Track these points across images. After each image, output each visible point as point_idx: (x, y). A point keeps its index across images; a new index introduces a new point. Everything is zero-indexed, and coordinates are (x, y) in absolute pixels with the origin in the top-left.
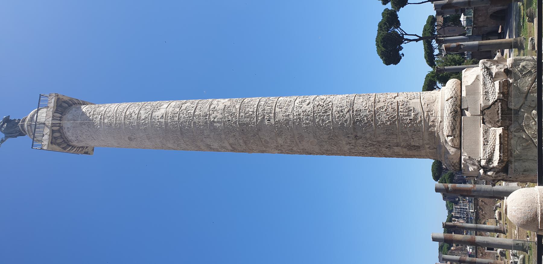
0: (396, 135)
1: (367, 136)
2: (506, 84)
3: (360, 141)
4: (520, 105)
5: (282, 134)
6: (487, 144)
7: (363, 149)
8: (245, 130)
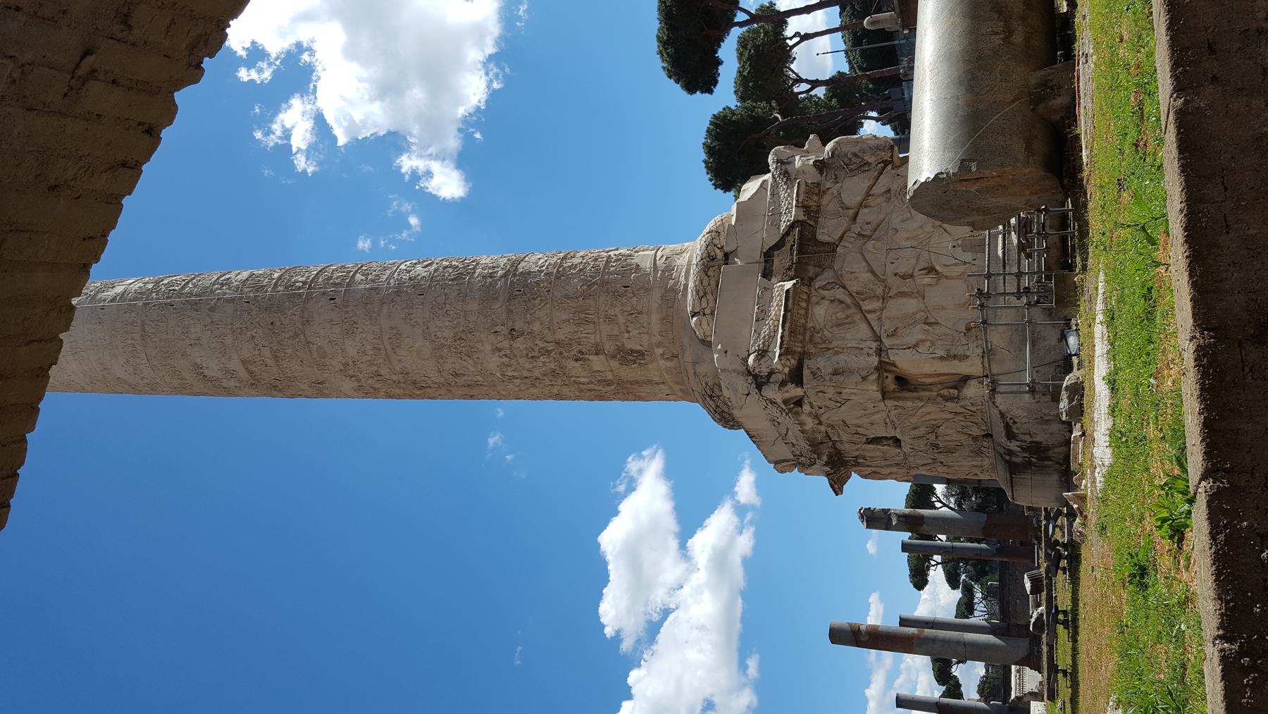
0: (594, 323)
1: (535, 329)
2: (817, 192)
3: (520, 344)
4: (841, 232)
5: (355, 330)
6: (763, 319)
7: (527, 366)
8: (278, 324)
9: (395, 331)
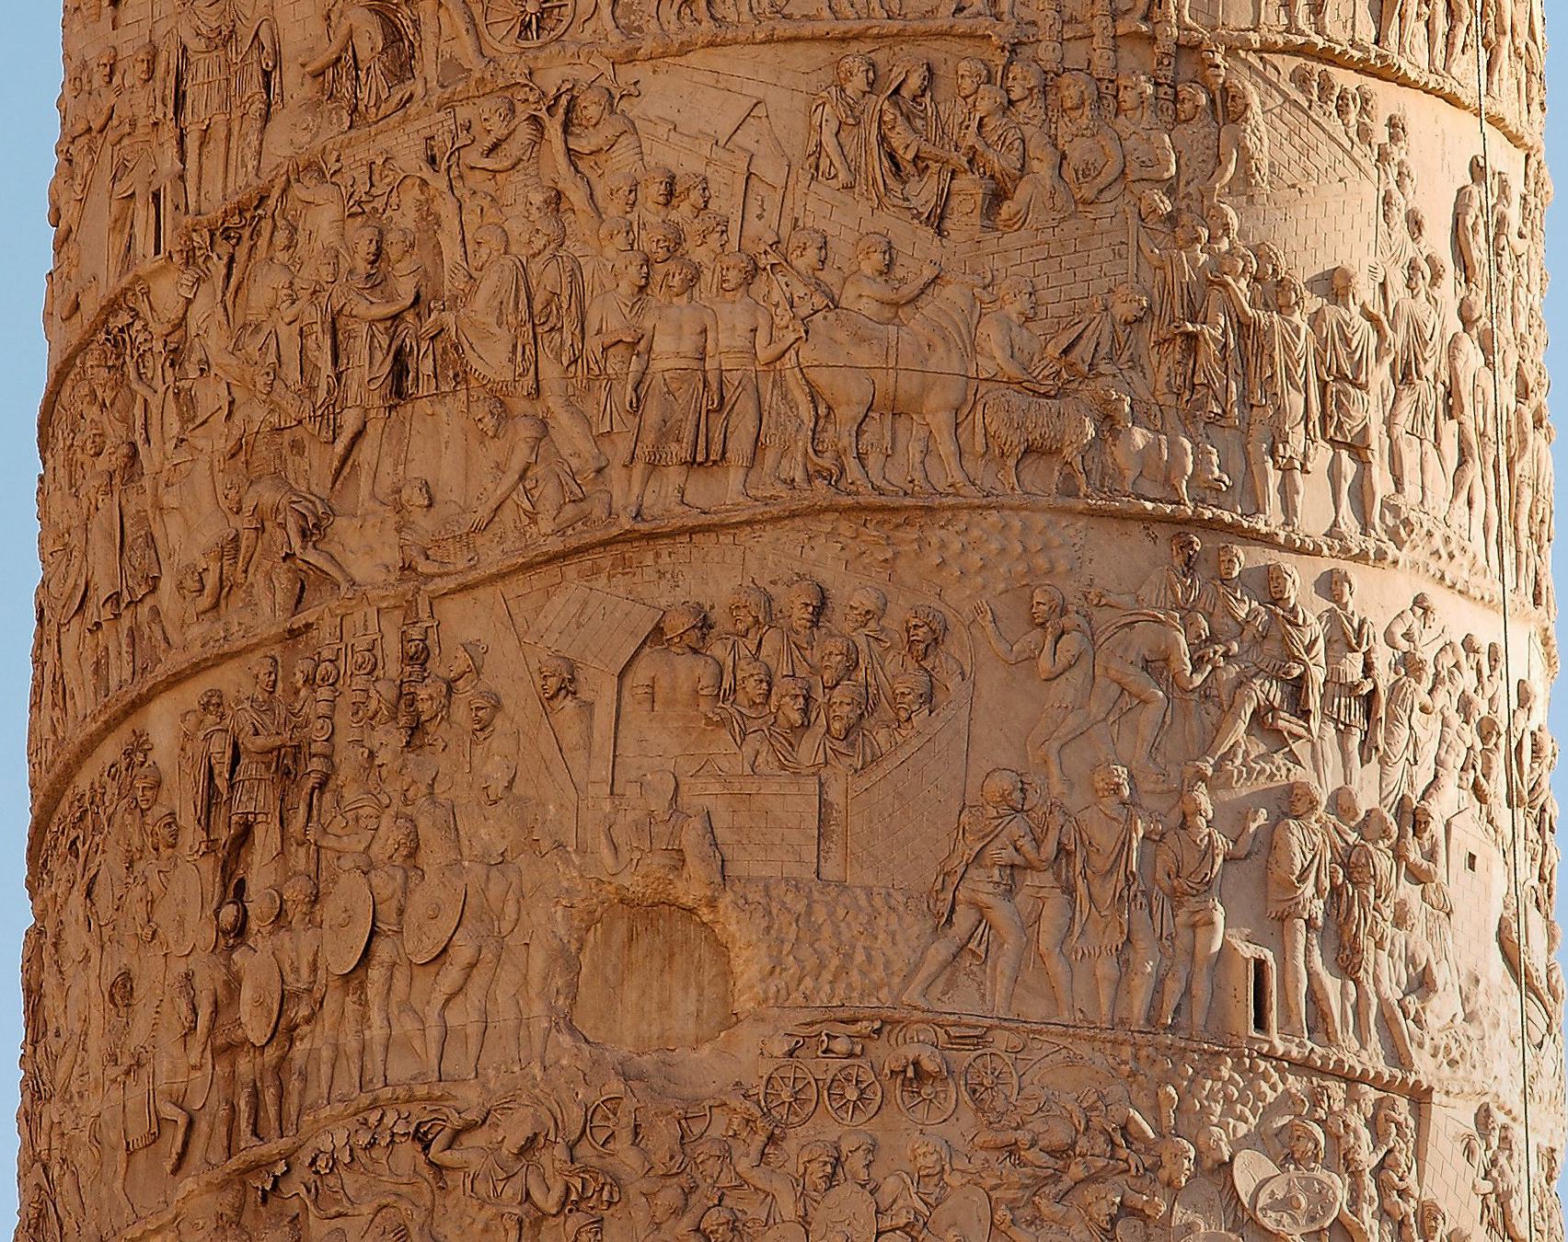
5: (924, 192)
9: (900, 675)
